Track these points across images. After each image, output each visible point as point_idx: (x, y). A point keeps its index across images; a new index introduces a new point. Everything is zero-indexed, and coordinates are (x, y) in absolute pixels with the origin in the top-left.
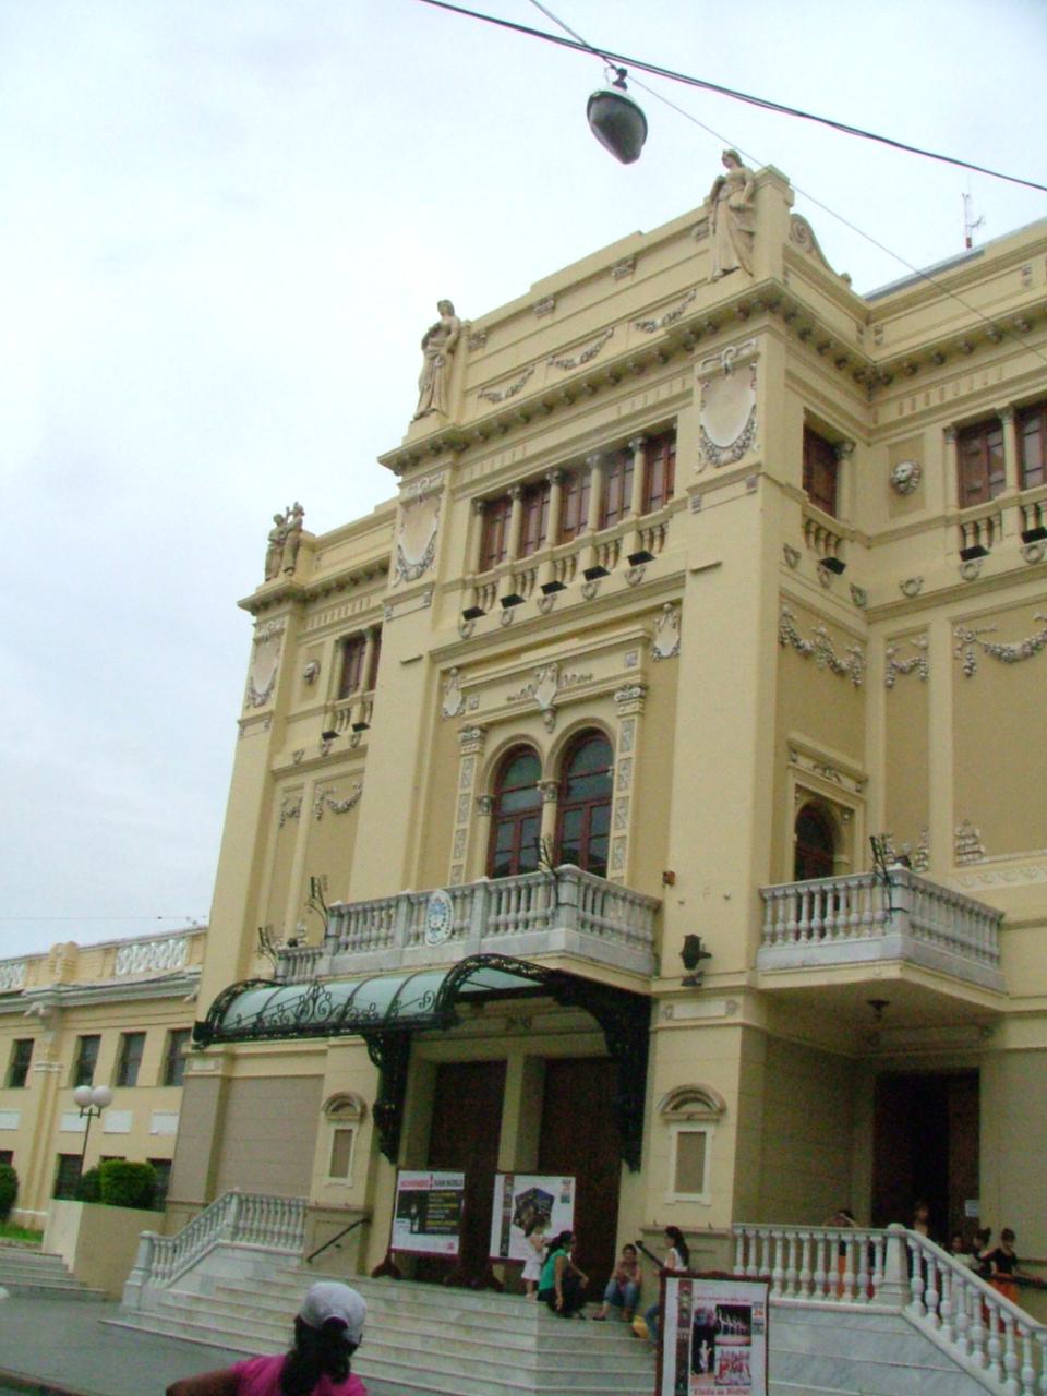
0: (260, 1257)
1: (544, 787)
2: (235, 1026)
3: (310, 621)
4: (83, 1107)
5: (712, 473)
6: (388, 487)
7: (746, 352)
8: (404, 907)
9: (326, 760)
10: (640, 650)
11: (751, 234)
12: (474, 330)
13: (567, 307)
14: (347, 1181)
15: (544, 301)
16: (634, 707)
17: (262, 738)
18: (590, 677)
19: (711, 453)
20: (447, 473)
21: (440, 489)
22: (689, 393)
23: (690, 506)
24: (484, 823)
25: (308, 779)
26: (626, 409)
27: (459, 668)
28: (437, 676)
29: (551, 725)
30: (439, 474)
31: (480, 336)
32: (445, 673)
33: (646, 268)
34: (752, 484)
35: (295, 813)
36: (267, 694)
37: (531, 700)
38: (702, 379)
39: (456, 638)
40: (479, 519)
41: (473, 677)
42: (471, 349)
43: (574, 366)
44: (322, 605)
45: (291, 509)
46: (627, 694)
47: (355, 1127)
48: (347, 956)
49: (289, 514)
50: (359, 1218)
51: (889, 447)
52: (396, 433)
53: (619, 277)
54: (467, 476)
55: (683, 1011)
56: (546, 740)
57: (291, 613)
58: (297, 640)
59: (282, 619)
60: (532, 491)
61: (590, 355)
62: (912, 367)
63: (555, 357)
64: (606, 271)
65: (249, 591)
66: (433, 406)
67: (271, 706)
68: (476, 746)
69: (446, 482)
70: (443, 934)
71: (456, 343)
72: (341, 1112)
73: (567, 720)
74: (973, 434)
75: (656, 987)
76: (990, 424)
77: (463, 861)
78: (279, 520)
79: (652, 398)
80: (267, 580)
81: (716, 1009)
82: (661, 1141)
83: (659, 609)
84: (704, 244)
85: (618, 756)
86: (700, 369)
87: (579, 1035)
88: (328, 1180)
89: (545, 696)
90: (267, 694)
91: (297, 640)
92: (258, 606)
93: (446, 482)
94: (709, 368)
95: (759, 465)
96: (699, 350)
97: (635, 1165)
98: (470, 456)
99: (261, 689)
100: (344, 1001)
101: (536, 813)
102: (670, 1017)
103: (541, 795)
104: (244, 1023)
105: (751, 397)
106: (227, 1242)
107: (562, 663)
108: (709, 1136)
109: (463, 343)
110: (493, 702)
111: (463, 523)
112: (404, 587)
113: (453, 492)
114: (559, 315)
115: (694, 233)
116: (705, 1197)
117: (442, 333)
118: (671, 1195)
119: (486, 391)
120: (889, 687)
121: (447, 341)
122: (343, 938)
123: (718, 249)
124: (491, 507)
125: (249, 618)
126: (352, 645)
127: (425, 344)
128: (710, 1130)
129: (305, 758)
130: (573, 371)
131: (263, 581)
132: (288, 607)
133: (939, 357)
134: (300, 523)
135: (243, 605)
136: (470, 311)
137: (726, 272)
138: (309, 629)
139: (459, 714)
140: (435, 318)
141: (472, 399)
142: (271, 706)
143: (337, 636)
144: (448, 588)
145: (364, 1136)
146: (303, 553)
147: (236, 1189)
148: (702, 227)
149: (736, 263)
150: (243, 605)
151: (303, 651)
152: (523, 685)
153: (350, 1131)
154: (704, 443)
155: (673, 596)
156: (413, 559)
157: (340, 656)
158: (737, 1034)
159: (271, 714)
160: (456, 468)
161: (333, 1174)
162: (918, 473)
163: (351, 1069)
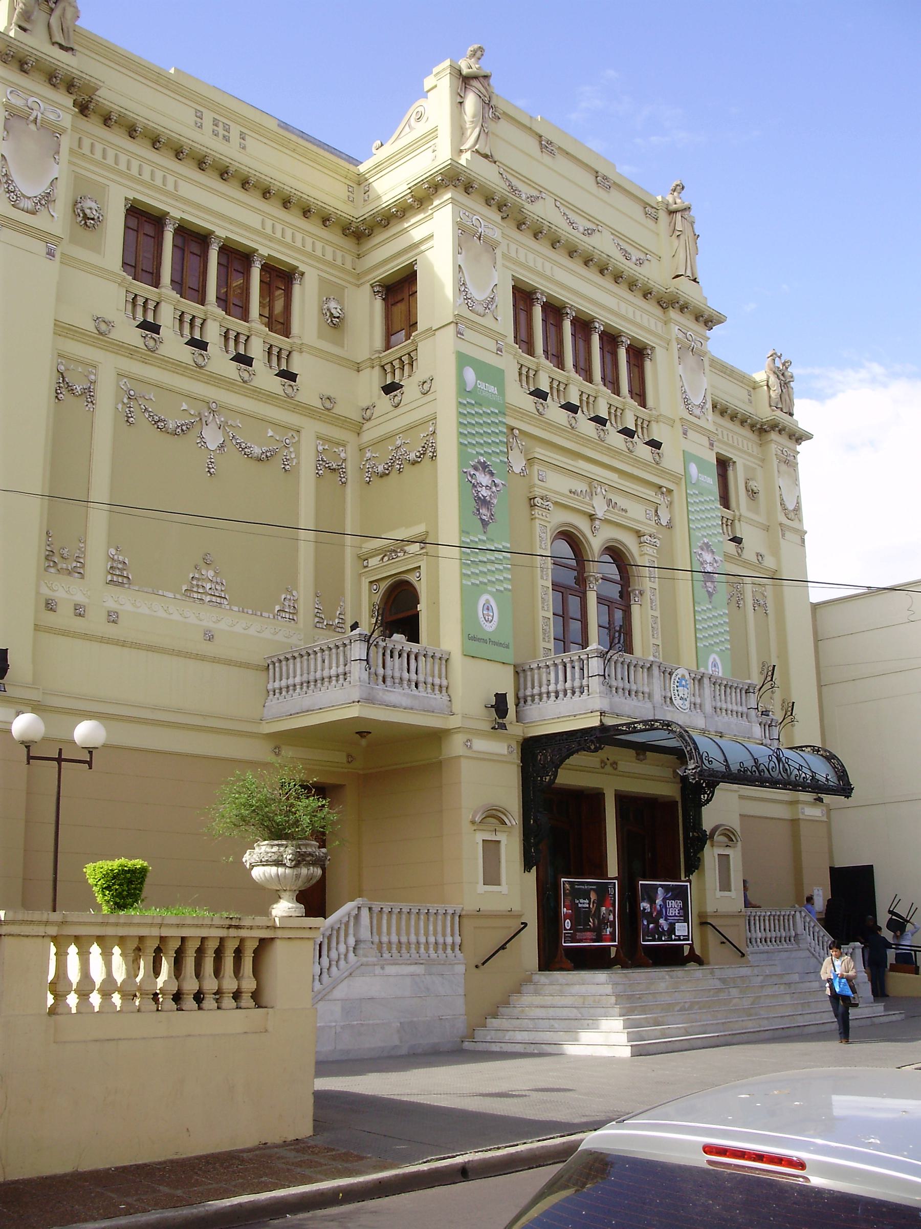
13: (562, 163)
35: (88, 394)
41: (540, 452)
83: (661, 487)
84: (650, 223)
87: (653, 781)
88: (481, 888)
130: (574, 232)
137: (695, 280)
153: (499, 842)
155: (671, 486)
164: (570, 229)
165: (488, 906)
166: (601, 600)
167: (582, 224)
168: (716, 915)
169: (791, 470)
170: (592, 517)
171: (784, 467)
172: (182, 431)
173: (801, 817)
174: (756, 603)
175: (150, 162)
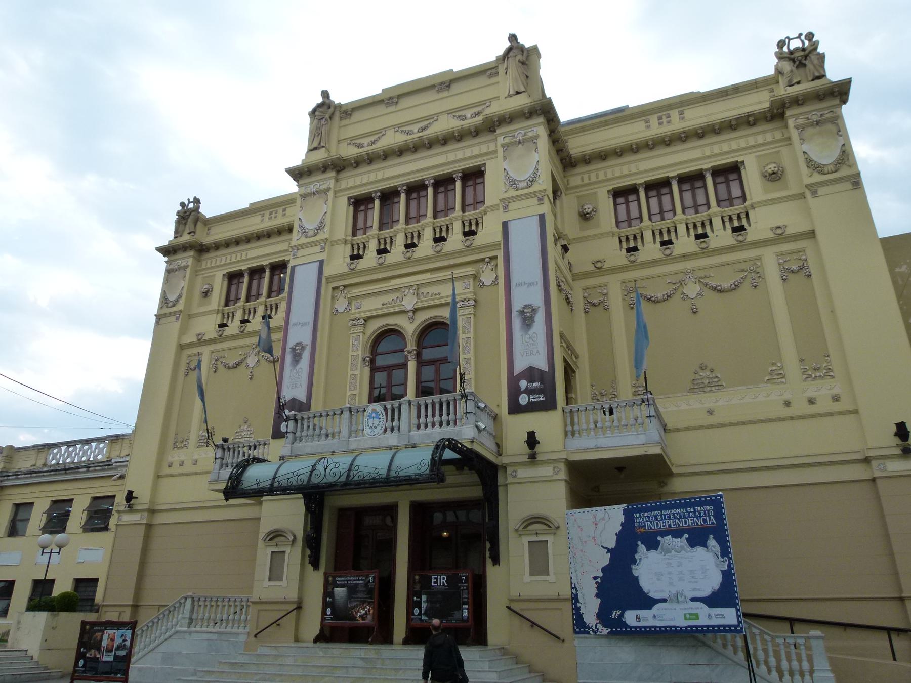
0: (215, 637)
1: (410, 352)
2: (255, 487)
3: (204, 263)
4: (43, 548)
5: (512, 193)
6: (290, 187)
7: (530, 134)
8: (346, 414)
9: (220, 338)
10: (471, 281)
11: (527, 77)
12: (343, 109)
14: (284, 583)
15: (391, 98)
16: (471, 310)
17: (174, 326)
18: (439, 294)
19: (513, 183)
20: (332, 182)
21: (328, 189)
22: (495, 152)
23: (501, 207)
24: (367, 370)
25: (206, 351)
26: (451, 157)
27: (345, 286)
28: (330, 290)
29: (412, 319)
30: (327, 180)
31: (349, 111)
32: (334, 289)
33: (455, 88)
34: (541, 200)
36: (177, 301)
37: (405, 304)
38: (503, 146)
39: (346, 269)
40: (351, 208)
41: (355, 291)
42: (341, 119)
43: (413, 133)
44: (213, 254)
45: (192, 200)
46: (466, 303)
47: (288, 550)
48: (301, 444)
49: (189, 203)
50: (295, 606)
51: (578, 197)
52: (298, 156)
53: (438, 91)
54: (343, 184)
55: (524, 473)
56: (410, 328)
57: (193, 257)
58: (196, 273)
59: (187, 259)
60: (388, 196)
61: (423, 129)
62: (587, 160)
63: (398, 127)
64: (433, 86)
65: (165, 243)
66: (322, 144)
67: (180, 307)
68: (361, 329)
69: (332, 186)
70: (379, 430)
71: (333, 114)
72: (276, 540)
73: (422, 318)
74: (622, 194)
75: (505, 460)
76: (632, 190)
77: (357, 392)
78: (182, 204)
79: (476, 151)
80: (175, 238)
81: (545, 471)
82: (515, 547)
83: (483, 260)
84: (494, 80)
85: (461, 336)
86: (500, 140)
88: (267, 583)
89: (409, 303)
90: (177, 301)
91: (196, 273)
92: (166, 251)
93: (332, 186)
94: (507, 140)
95: (545, 190)
96: (499, 131)
97: (496, 560)
98: (343, 175)
99: (172, 298)
100: (347, 467)
101: (404, 366)
102: (515, 477)
103: (406, 356)
104: (262, 485)
105: (536, 157)
106: (185, 629)
107: (419, 286)
108: (550, 544)
109: (337, 114)
110: (371, 305)
111: (344, 211)
112: (304, 240)
113: (335, 192)
114: (399, 107)
115: (489, 72)
116: (552, 578)
117: (326, 107)
118: (527, 578)
119: (352, 141)
120: (586, 312)
121: (326, 113)
122: (298, 434)
123: (507, 82)
124: (360, 203)
125: (162, 259)
126: (233, 277)
127: (313, 113)
128: (550, 539)
129: (205, 338)
130: (413, 136)
131: (172, 238)
132: (192, 253)
133: (603, 156)
134: (199, 208)
135: (159, 250)
136: (339, 97)
137: (518, 93)
138: (203, 267)
139: (347, 311)
140: (320, 100)
141: (344, 145)
142: (180, 307)
143: (225, 272)
144: (333, 243)
145: (294, 555)
146: (199, 224)
147: (190, 594)
148: (494, 71)
149: (523, 89)
150: (159, 250)
151: (199, 280)
152: (394, 296)
154: (508, 177)
155: (492, 254)
156: (310, 226)
157: (226, 282)
158: (563, 484)
159: (181, 311)
160: (337, 180)
161: (270, 580)
162: (595, 210)
163: (289, 514)
164: (409, 137)
165: (265, 596)
166: (421, 363)
167: (415, 128)
168: (520, 600)
169: (830, 127)
170: (404, 312)
171: (810, 131)
172: (238, 365)
173: (877, 474)
174: (786, 274)
175: (624, 164)
